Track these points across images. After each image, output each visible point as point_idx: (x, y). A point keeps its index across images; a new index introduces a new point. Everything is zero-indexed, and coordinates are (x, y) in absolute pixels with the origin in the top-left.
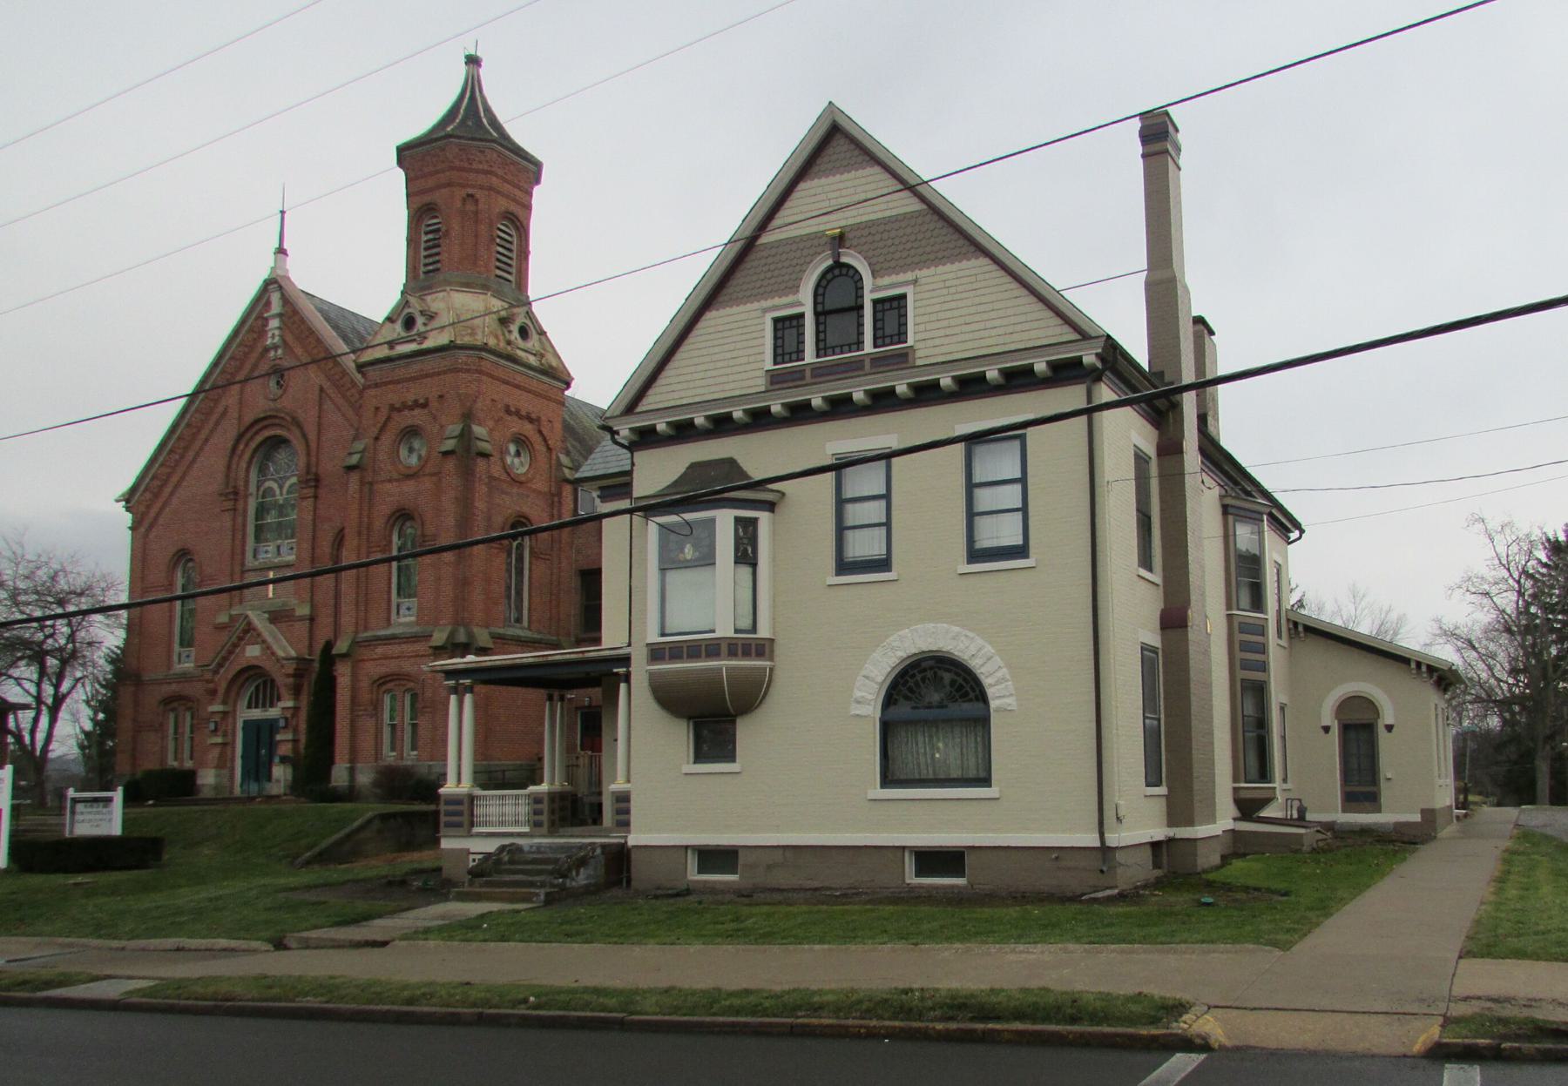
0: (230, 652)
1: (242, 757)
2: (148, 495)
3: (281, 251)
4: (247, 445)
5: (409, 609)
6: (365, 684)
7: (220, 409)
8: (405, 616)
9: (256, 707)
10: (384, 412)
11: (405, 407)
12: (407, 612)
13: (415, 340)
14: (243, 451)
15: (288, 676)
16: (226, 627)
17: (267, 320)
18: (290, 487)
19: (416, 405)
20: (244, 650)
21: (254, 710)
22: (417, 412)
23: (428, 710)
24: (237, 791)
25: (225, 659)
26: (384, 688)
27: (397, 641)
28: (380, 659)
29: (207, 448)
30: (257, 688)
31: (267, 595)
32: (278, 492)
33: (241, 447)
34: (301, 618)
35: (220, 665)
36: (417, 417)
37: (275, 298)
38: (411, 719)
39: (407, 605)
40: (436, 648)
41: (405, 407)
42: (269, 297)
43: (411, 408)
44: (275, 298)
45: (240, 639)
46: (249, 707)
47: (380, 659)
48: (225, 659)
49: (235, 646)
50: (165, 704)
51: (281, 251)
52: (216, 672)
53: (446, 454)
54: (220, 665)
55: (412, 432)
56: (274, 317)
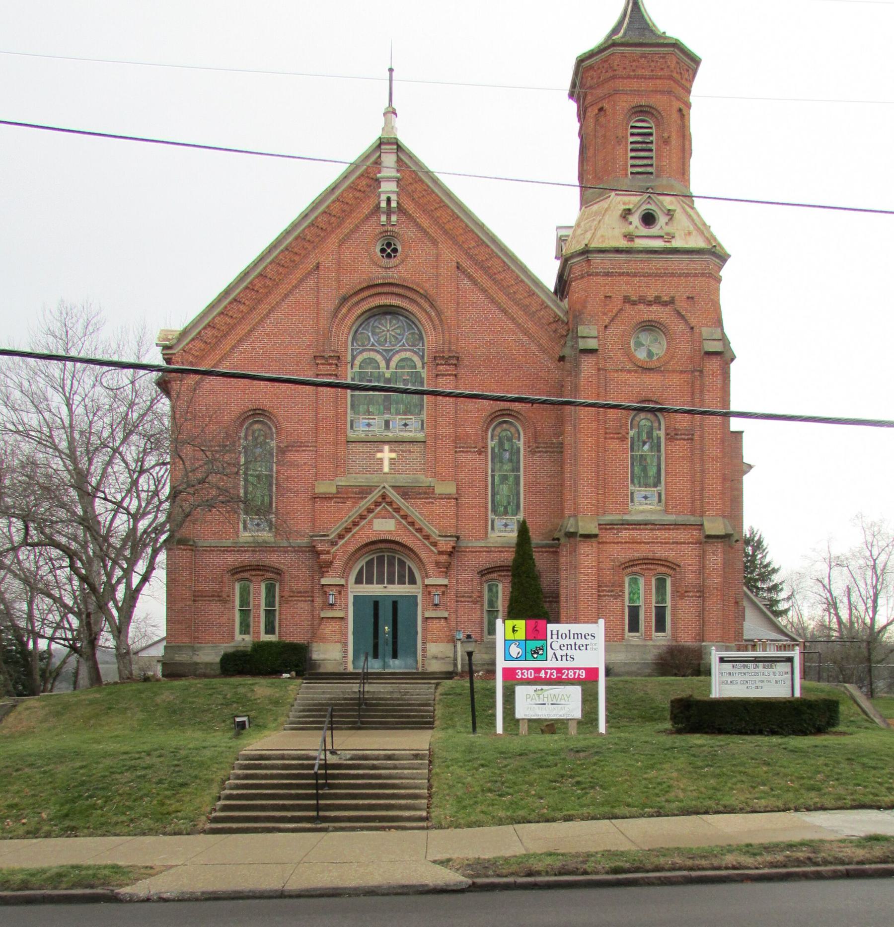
0: (355, 524)
1: (354, 633)
2: (199, 344)
3: (391, 112)
4: (349, 310)
5: (646, 498)
6: (607, 565)
7: (311, 263)
8: (641, 504)
9: (393, 583)
10: (617, 303)
11: (642, 300)
12: (643, 501)
13: (662, 237)
14: (345, 316)
15: (441, 553)
16: (331, 498)
17: (378, 181)
18: (402, 360)
19: (658, 301)
20: (371, 523)
21: (364, 585)
22: (654, 308)
23: (691, 594)
24: (350, 668)
25: (348, 530)
26: (629, 570)
27: (649, 527)
28: (626, 543)
29: (284, 305)
30: (369, 564)
31: (381, 469)
32: (383, 364)
33: (344, 311)
34: (448, 497)
35: (341, 537)
36: (657, 313)
37: (389, 160)
38: (657, 603)
39: (643, 494)
40: (709, 537)
41: (642, 300)
42: (380, 157)
43: (650, 304)
44: (389, 160)
45: (370, 511)
46: (358, 581)
47: (626, 543)
48: (348, 530)
49: (362, 517)
50: (233, 575)
51: (391, 112)
52: (334, 543)
53: (709, 354)
54: (341, 537)
55: (649, 326)
56: (389, 179)
